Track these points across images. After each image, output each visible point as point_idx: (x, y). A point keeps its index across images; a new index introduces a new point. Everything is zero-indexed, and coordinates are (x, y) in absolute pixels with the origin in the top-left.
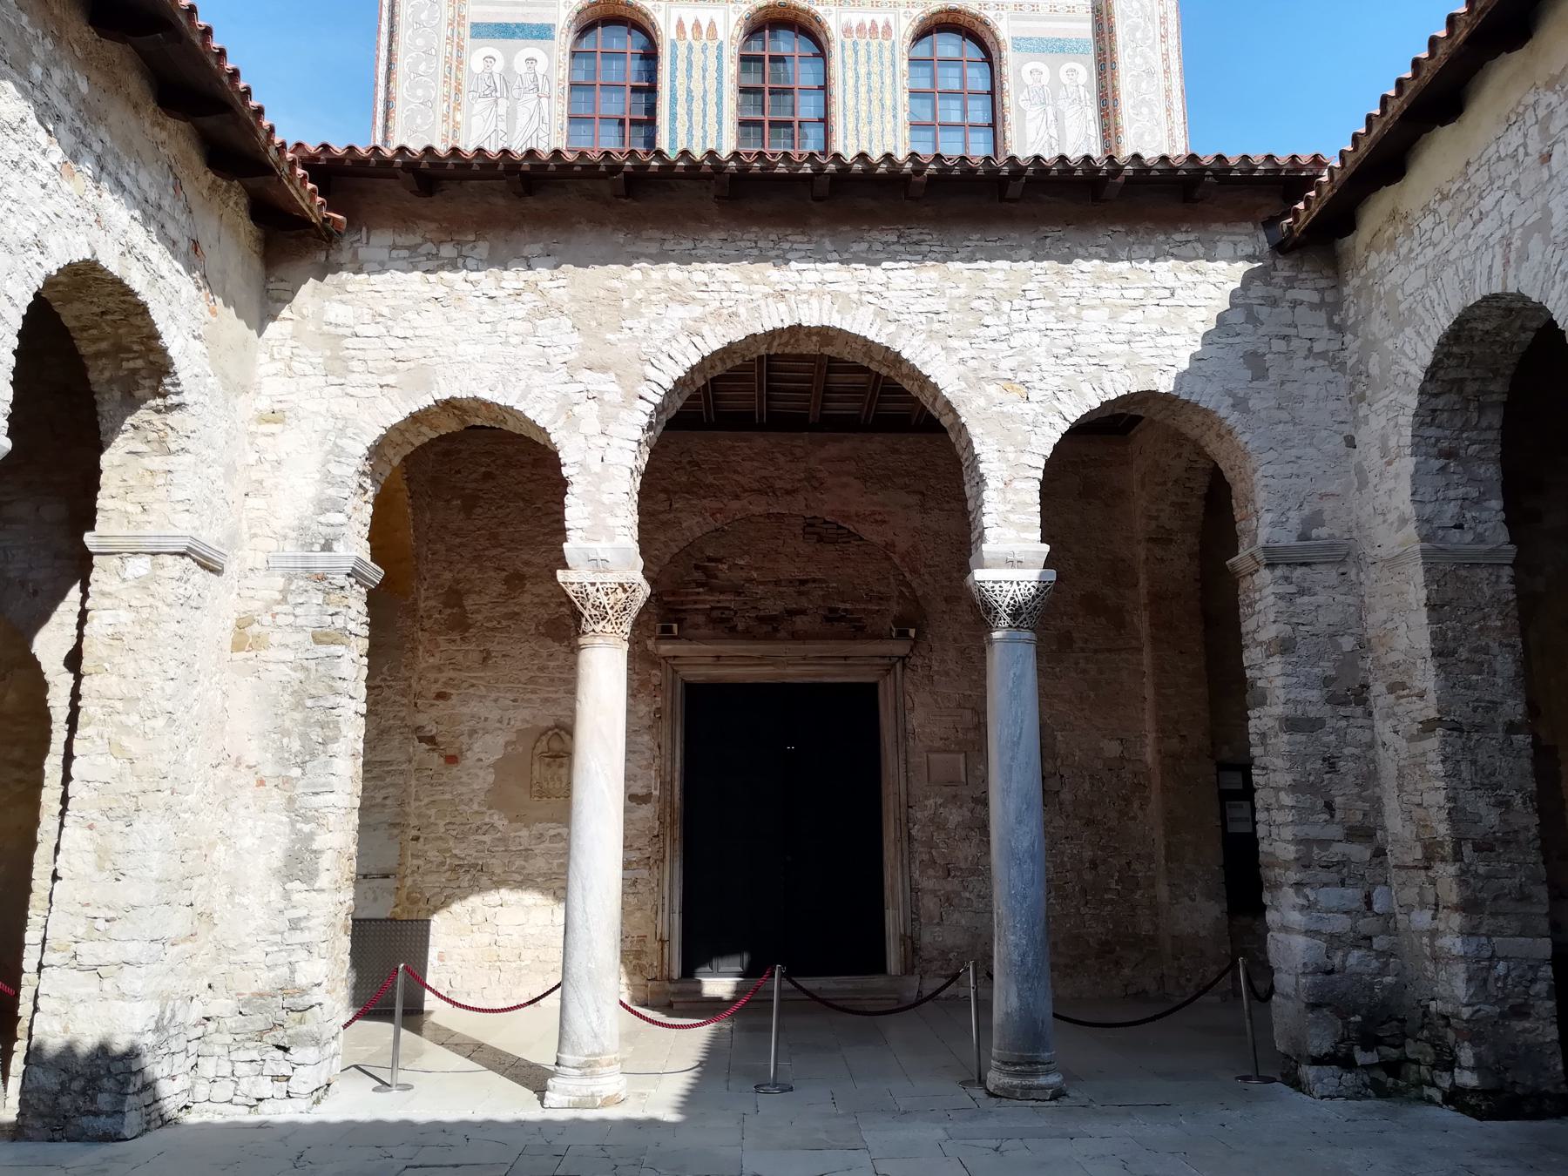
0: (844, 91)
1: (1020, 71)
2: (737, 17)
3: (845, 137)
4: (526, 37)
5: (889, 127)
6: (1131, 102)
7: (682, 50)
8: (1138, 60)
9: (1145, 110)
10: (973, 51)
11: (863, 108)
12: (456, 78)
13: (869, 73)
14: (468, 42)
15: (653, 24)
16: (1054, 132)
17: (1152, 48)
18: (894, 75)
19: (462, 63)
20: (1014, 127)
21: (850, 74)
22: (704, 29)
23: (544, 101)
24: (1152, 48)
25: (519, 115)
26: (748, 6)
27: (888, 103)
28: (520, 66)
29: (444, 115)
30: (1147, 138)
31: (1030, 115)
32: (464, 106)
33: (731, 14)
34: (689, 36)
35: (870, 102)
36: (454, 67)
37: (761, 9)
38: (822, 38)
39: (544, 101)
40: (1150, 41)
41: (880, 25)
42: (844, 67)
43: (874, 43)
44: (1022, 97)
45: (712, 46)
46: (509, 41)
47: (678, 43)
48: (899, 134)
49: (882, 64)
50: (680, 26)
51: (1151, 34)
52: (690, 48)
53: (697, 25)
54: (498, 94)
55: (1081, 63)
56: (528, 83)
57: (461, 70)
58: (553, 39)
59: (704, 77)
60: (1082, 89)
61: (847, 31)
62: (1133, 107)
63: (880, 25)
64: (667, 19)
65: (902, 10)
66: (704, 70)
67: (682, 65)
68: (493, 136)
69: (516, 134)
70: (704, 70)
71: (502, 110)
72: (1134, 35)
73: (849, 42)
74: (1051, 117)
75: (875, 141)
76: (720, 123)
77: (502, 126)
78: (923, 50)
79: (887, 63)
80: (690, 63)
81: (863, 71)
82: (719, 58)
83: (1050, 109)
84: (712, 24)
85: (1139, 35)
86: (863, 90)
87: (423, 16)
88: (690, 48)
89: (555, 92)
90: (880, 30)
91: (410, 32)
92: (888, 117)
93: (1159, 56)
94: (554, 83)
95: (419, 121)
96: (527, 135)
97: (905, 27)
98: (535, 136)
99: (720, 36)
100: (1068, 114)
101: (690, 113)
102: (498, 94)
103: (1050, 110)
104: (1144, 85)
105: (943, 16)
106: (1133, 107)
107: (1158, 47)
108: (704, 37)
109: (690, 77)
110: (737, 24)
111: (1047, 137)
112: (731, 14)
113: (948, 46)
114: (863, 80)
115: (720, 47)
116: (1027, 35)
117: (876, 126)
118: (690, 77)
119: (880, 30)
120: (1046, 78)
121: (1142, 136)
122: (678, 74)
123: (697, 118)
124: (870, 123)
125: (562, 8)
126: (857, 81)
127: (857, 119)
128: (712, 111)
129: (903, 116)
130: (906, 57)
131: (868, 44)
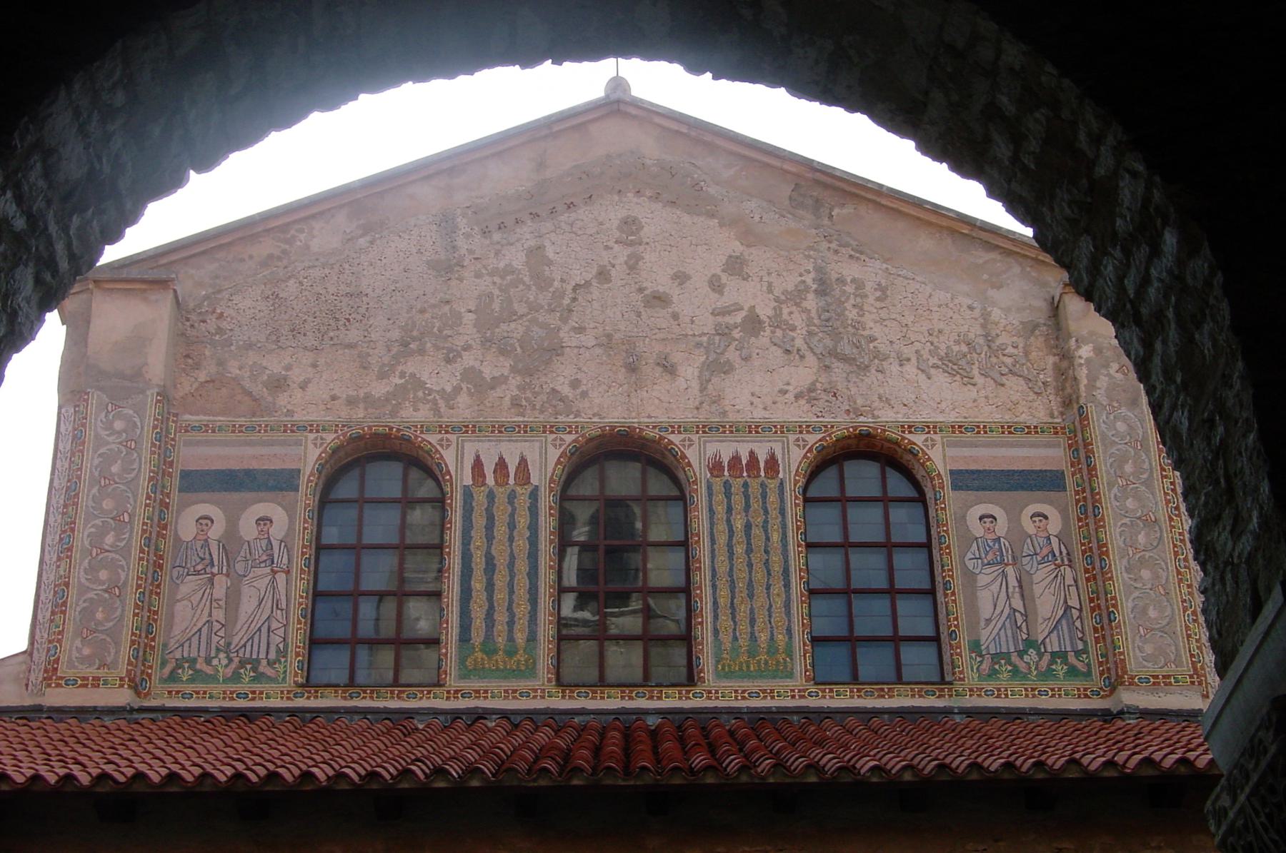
0: (713, 551)
1: (964, 517)
2: (558, 452)
3: (716, 617)
4: (259, 489)
5: (779, 602)
6: (1125, 562)
7: (480, 498)
8: (1130, 503)
9: (1145, 574)
10: (898, 485)
11: (741, 575)
12: (157, 549)
13: (748, 527)
14: (175, 496)
15: (439, 465)
16: (1017, 603)
17: (1148, 483)
18: (784, 526)
19: (165, 527)
20: (960, 598)
21: (722, 527)
22: (512, 470)
23: (281, 578)
24: (1148, 483)
25: (244, 599)
26: (573, 437)
27: (777, 568)
28: (247, 528)
29: (136, 606)
30: (1152, 613)
31: (983, 580)
32: (165, 589)
33: (551, 449)
34: (490, 480)
35: (750, 565)
36: (154, 536)
37: (591, 439)
38: (681, 476)
39: (281, 578)
40: (1145, 476)
41: (762, 458)
42: (711, 518)
43: (754, 485)
44: (970, 555)
45: (523, 493)
46: (236, 496)
47: (475, 490)
48: (794, 611)
49: (766, 512)
50: (478, 465)
51: (1146, 466)
52: (491, 496)
53: (501, 465)
54: (215, 570)
55: (1051, 503)
56: (259, 554)
57: (164, 537)
58: (297, 490)
59: (511, 539)
60: (1055, 541)
61: (716, 467)
62: (1128, 570)
63: (762, 458)
64: (460, 458)
65: (792, 437)
66: (512, 526)
67: (479, 521)
68: (205, 630)
69: (238, 627)
70: (512, 526)
71: (219, 592)
72: (1121, 467)
73: (718, 484)
74: (1013, 582)
75: (759, 621)
76: (534, 601)
77: (219, 615)
78: (827, 485)
79: (774, 513)
80: (491, 519)
81: (739, 524)
82: (534, 510)
83: (1010, 571)
84: (523, 462)
85: (1128, 468)
86: (740, 550)
87: (115, 469)
88: (491, 496)
89: (298, 562)
90: (762, 465)
91: (95, 491)
92: (777, 588)
93: (1160, 496)
94: (297, 552)
95: (99, 616)
96: (254, 627)
97: (794, 459)
98: (264, 630)
99: (535, 480)
100: (1036, 578)
101: (490, 587)
102: (215, 570)
103: (1010, 571)
104: (1141, 538)
105: (850, 441)
106: (1128, 570)
107: (1157, 484)
108: (512, 481)
109: (490, 537)
110: (558, 462)
111: (1007, 611)
112: (551, 449)
113: (863, 478)
114: (739, 535)
115: (534, 495)
116: (973, 467)
117: (761, 600)
118: (490, 537)
119: (762, 465)
120: (1002, 527)
121: (1144, 611)
122: (473, 533)
123: (500, 596)
124: (751, 596)
125: (311, 446)
126: (731, 537)
127: (733, 592)
128: (522, 583)
129: (797, 588)
130: (800, 501)
131: (746, 485)
